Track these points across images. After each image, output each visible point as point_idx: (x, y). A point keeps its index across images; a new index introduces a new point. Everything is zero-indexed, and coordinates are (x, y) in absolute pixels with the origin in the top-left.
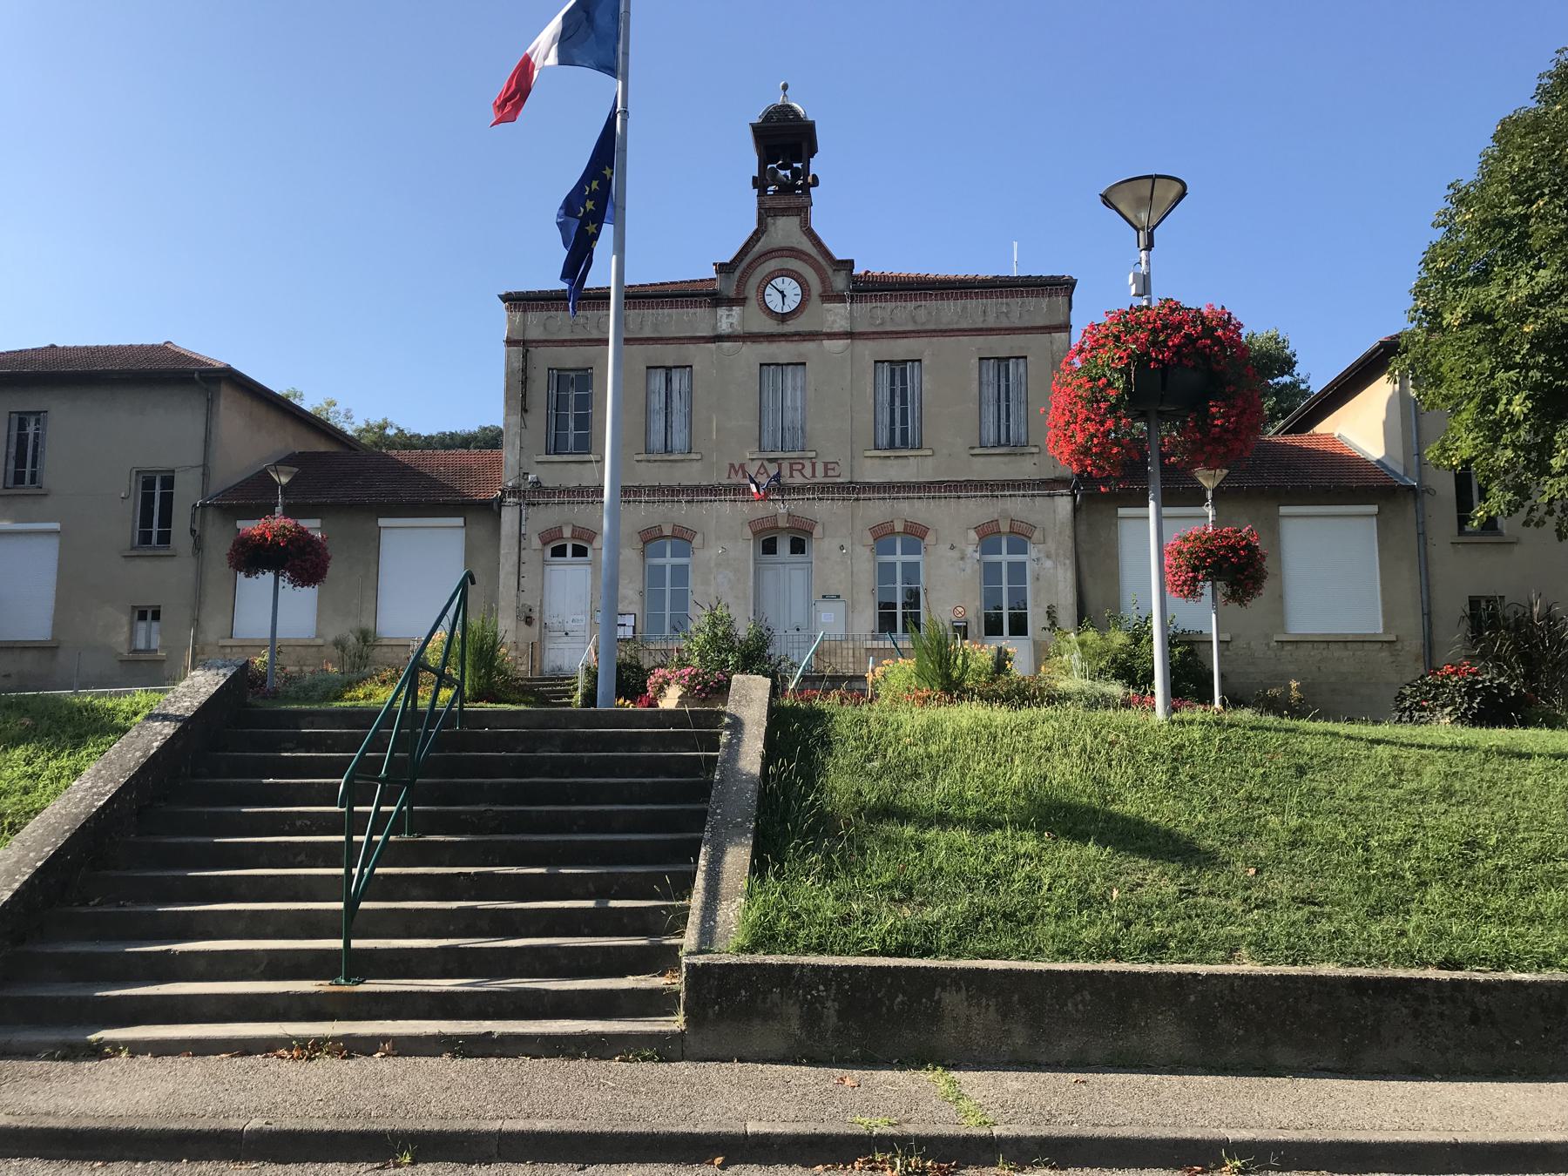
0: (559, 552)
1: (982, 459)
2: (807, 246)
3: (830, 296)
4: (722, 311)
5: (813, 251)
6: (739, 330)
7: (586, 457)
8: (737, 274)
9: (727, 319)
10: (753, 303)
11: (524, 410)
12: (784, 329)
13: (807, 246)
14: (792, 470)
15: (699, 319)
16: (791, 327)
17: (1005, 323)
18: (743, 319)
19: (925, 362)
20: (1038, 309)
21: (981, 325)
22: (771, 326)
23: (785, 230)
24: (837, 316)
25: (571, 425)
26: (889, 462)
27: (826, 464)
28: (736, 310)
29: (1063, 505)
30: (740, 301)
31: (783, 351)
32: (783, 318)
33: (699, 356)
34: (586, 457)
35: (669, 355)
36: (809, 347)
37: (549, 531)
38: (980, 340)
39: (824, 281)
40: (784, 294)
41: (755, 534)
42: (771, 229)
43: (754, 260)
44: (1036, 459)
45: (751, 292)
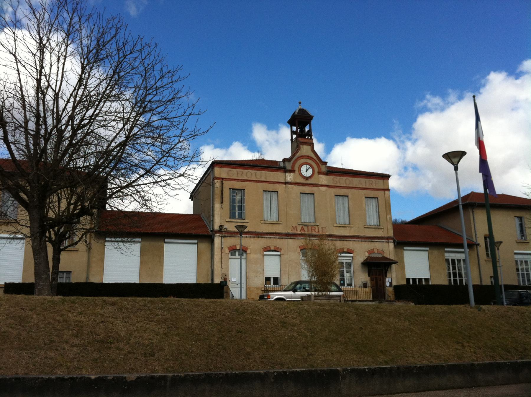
0: (233, 254)
1: (368, 229)
2: (313, 156)
3: (320, 173)
4: (287, 174)
5: (315, 158)
6: (293, 181)
7: (244, 221)
8: (292, 162)
9: (290, 177)
10: (297, 172)
11: (222, 203)
12: (306, 182)
13: (313, 156)
14: (312, 229)
15: (279, 176)
16: (309, 182)
17: (371, 187)
18: (294, 177)
19: (350, 197)
20: (380, 183)
21: (364, 187)
22: (303, 181)
23: (305, 150)
24: (324, 179)
25: (237, 209)
26: (341, 228)
27: (322, 228)
28: (292, 174)
29: (392, 245)
30: (292, 171)
31: (307, 189)
32: (307, 178)
33: (281, 188)
34: (244, 221)
35: (270, 187)
36: (315, 189)
37: (232, 247)
38: (365, 191)
39: (319, 167)
40: (306, 171)
41: (301, 250)
42: (302, 149)
43: (297, 158)
44: (383, 230)
45: (296, 168)
